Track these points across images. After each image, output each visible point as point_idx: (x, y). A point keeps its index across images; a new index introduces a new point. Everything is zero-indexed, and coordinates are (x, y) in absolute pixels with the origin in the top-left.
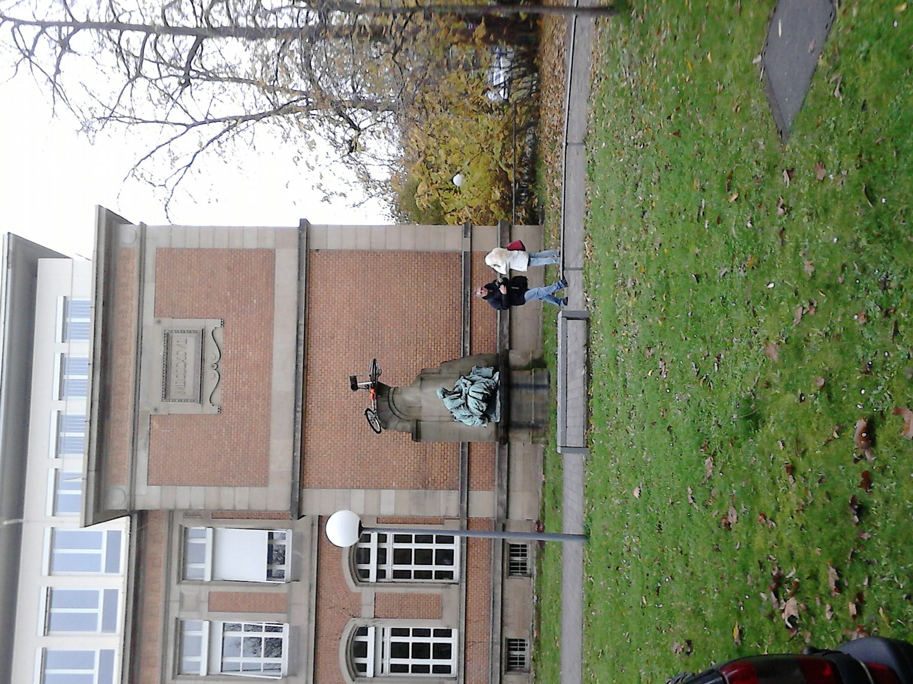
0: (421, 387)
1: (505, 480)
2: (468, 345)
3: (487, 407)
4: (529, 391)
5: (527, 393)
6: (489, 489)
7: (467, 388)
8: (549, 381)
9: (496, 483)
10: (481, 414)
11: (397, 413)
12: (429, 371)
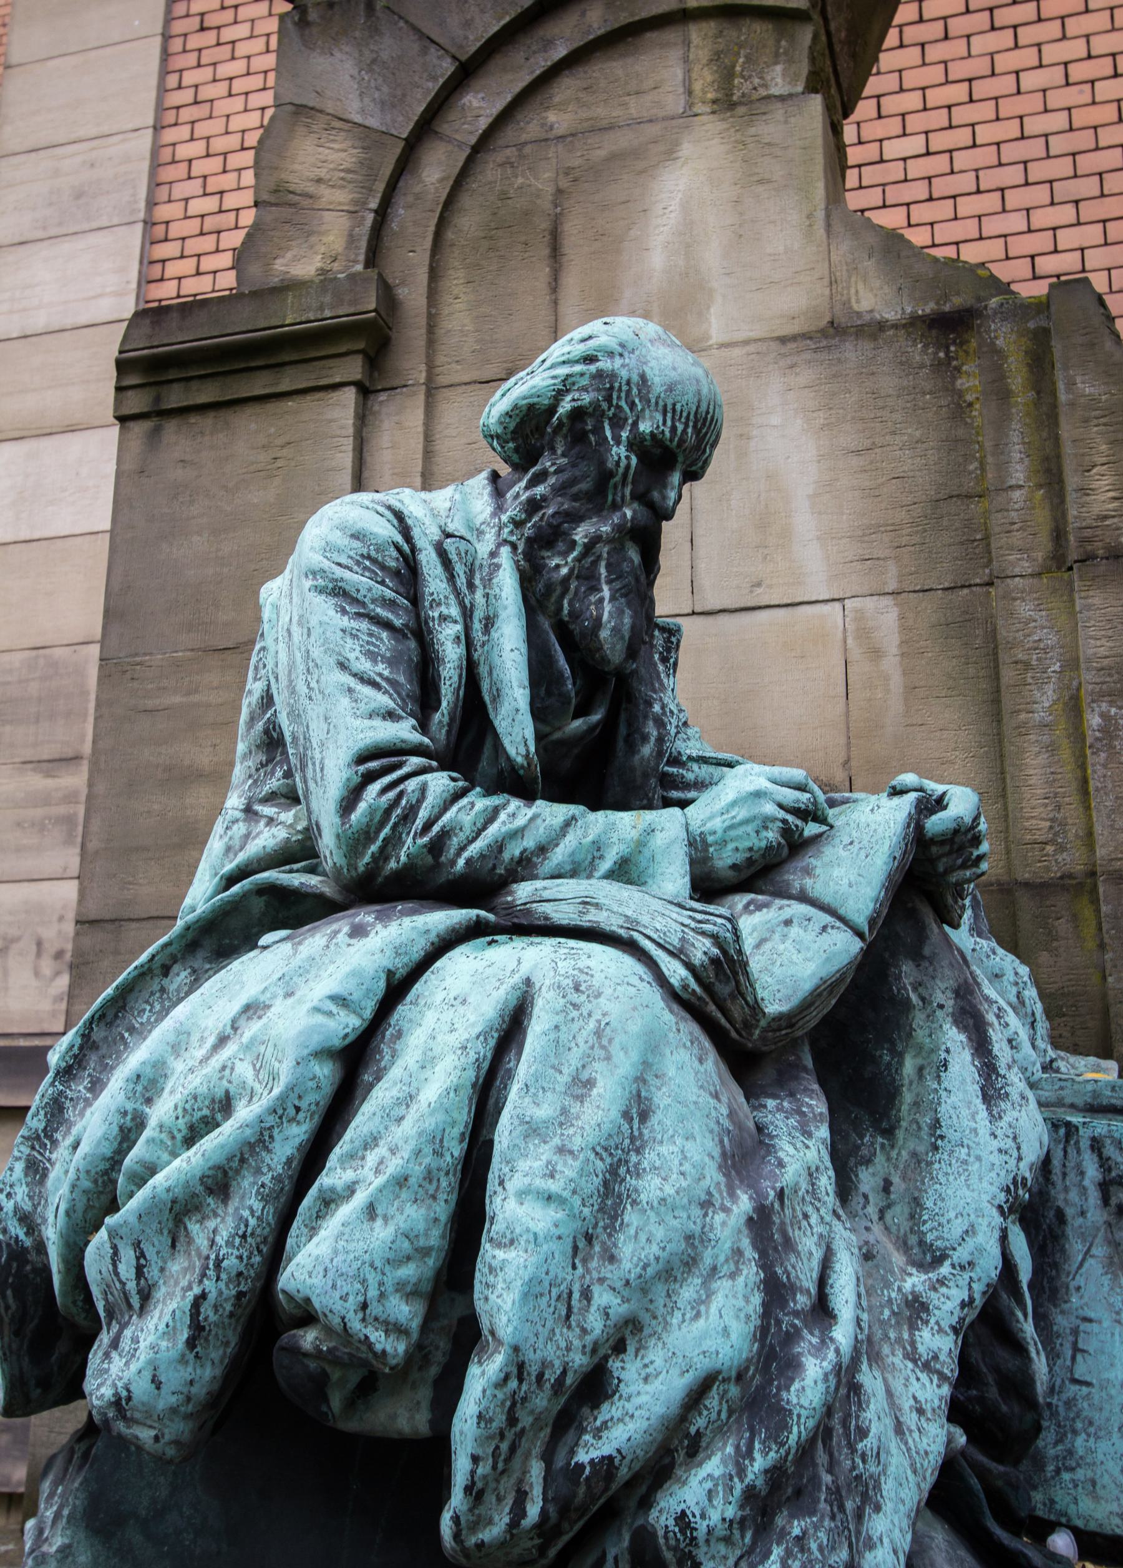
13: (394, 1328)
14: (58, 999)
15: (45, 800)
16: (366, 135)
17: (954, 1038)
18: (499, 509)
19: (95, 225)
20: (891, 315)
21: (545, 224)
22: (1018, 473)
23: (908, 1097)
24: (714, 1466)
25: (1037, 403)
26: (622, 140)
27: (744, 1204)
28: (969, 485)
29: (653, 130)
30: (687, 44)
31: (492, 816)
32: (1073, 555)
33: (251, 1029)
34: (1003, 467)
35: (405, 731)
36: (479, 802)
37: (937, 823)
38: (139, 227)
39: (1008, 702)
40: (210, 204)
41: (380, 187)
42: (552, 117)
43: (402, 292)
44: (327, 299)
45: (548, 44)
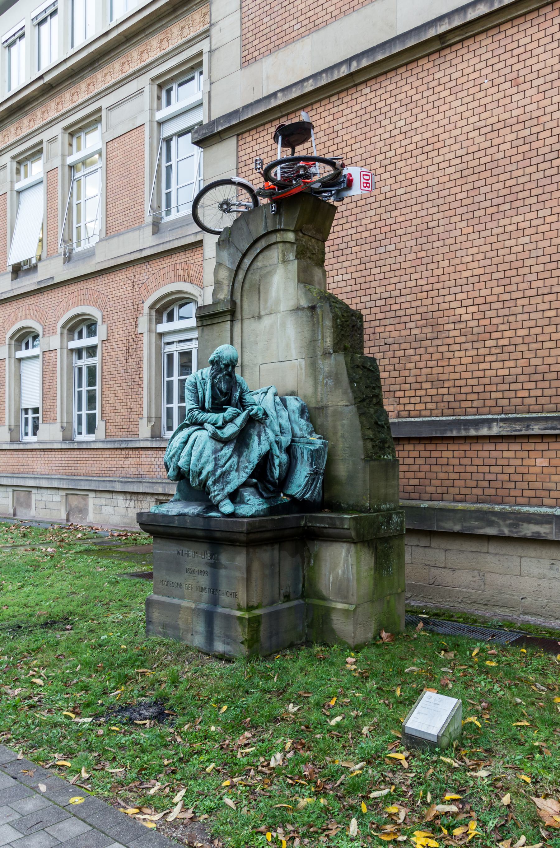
0: (298, 309)
2: (495, 430)
4: (205, 595)
5: (203, 589)
8: (221, 657)
16: (230, 270)
17: (256, 438)
20: (305, 306)
22: (320, 338)
26: (268, 269)
29: (273, 267)
35: (194, 406)
37: (251, 413)
42: (258, 264)
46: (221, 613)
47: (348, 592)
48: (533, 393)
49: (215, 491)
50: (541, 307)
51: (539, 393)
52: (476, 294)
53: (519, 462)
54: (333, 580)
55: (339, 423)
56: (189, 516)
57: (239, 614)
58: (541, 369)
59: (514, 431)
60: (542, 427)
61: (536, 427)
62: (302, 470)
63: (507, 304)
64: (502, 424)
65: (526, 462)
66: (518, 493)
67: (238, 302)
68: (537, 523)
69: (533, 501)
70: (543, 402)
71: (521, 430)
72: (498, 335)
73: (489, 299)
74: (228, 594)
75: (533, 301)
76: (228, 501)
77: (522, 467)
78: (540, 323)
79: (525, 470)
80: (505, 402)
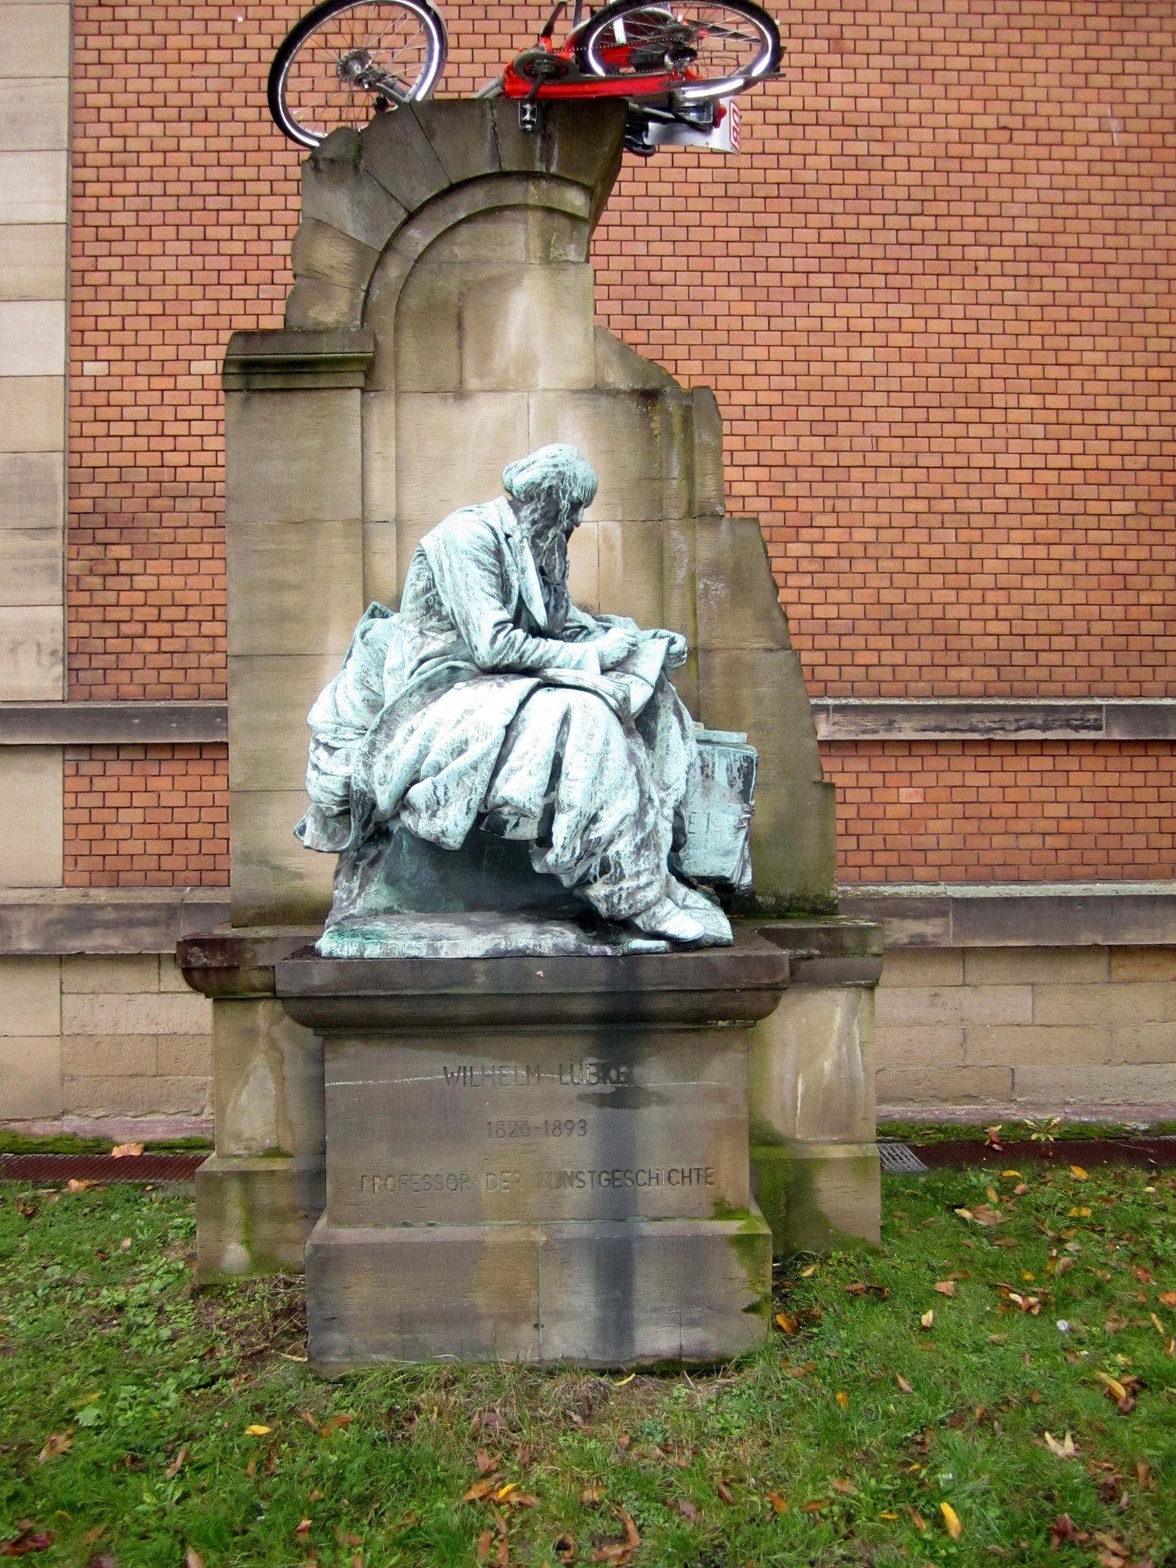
0: (597, 390)
1: (114, 942)
3: (432, 848)
4: (578, 1196)
5: (564, 1179)
6: (71, 858)
7: (591, 676)
9: (102, 895)
10: (384, 800)
11: (418, 237)
12: (703, 437)
13: (536, 805)
14: (56, 680)
15: (33, 555)
16: (360, 249)
17: (674, 719)
18: (519, 522)
19: (29, 146)
21: (454, 311)
22: (676, 471)
23: (659, 738)
24: (627, 838)
25: (685, 440)
27: (634, 769)
28: (654, 474)
30: (526, 221)
31: (538, 647)
32: (697, 513)
33: (470, 718)
34: (669, 469)
36: (532, 642)
37: (675, 649)
38: (64, 154)
39: (667, 574)
40: (117, 144)
41: (368, 278)
42: (457, 250)
43: (380, 338)
44: (346, 341)
45: (455, 209)
46: (662, 1240)
47: (851, 1112)
48: (887, 658)
49: (638, 874)
50: (898, 490)
51: (898, 658)
52: (764, 443)
53: (865, 795)
54: (807, 1089)
55: (746, 692)
56: (541, 956)
57: (732, 1227)
58: (900, 610)
59: (864, 732)
60: (919, 725)
61: (905, 725)
62: (714, 812)
63: (830, 474)
64: (837, 717)
65: (880, 795)
66: (864, 858)
67: (386, 340)
68: (918, 916)
69: (894, 873)
70: (907, 677)
71: (876, 732)
72: (814, 534)
73: (792, 458)
74: (676, 1177)
75: (883, 475)
76: (669, 904)
77: (872, 806)
78: (898, 521)
79: (878, 813)
80: (832, 673)
